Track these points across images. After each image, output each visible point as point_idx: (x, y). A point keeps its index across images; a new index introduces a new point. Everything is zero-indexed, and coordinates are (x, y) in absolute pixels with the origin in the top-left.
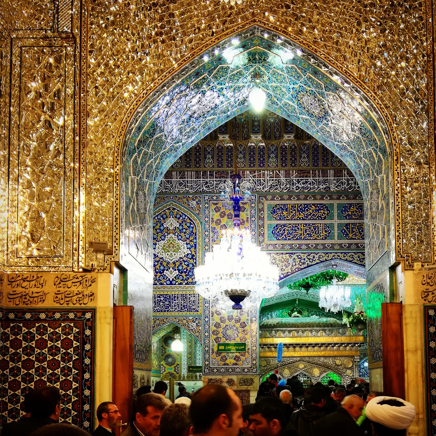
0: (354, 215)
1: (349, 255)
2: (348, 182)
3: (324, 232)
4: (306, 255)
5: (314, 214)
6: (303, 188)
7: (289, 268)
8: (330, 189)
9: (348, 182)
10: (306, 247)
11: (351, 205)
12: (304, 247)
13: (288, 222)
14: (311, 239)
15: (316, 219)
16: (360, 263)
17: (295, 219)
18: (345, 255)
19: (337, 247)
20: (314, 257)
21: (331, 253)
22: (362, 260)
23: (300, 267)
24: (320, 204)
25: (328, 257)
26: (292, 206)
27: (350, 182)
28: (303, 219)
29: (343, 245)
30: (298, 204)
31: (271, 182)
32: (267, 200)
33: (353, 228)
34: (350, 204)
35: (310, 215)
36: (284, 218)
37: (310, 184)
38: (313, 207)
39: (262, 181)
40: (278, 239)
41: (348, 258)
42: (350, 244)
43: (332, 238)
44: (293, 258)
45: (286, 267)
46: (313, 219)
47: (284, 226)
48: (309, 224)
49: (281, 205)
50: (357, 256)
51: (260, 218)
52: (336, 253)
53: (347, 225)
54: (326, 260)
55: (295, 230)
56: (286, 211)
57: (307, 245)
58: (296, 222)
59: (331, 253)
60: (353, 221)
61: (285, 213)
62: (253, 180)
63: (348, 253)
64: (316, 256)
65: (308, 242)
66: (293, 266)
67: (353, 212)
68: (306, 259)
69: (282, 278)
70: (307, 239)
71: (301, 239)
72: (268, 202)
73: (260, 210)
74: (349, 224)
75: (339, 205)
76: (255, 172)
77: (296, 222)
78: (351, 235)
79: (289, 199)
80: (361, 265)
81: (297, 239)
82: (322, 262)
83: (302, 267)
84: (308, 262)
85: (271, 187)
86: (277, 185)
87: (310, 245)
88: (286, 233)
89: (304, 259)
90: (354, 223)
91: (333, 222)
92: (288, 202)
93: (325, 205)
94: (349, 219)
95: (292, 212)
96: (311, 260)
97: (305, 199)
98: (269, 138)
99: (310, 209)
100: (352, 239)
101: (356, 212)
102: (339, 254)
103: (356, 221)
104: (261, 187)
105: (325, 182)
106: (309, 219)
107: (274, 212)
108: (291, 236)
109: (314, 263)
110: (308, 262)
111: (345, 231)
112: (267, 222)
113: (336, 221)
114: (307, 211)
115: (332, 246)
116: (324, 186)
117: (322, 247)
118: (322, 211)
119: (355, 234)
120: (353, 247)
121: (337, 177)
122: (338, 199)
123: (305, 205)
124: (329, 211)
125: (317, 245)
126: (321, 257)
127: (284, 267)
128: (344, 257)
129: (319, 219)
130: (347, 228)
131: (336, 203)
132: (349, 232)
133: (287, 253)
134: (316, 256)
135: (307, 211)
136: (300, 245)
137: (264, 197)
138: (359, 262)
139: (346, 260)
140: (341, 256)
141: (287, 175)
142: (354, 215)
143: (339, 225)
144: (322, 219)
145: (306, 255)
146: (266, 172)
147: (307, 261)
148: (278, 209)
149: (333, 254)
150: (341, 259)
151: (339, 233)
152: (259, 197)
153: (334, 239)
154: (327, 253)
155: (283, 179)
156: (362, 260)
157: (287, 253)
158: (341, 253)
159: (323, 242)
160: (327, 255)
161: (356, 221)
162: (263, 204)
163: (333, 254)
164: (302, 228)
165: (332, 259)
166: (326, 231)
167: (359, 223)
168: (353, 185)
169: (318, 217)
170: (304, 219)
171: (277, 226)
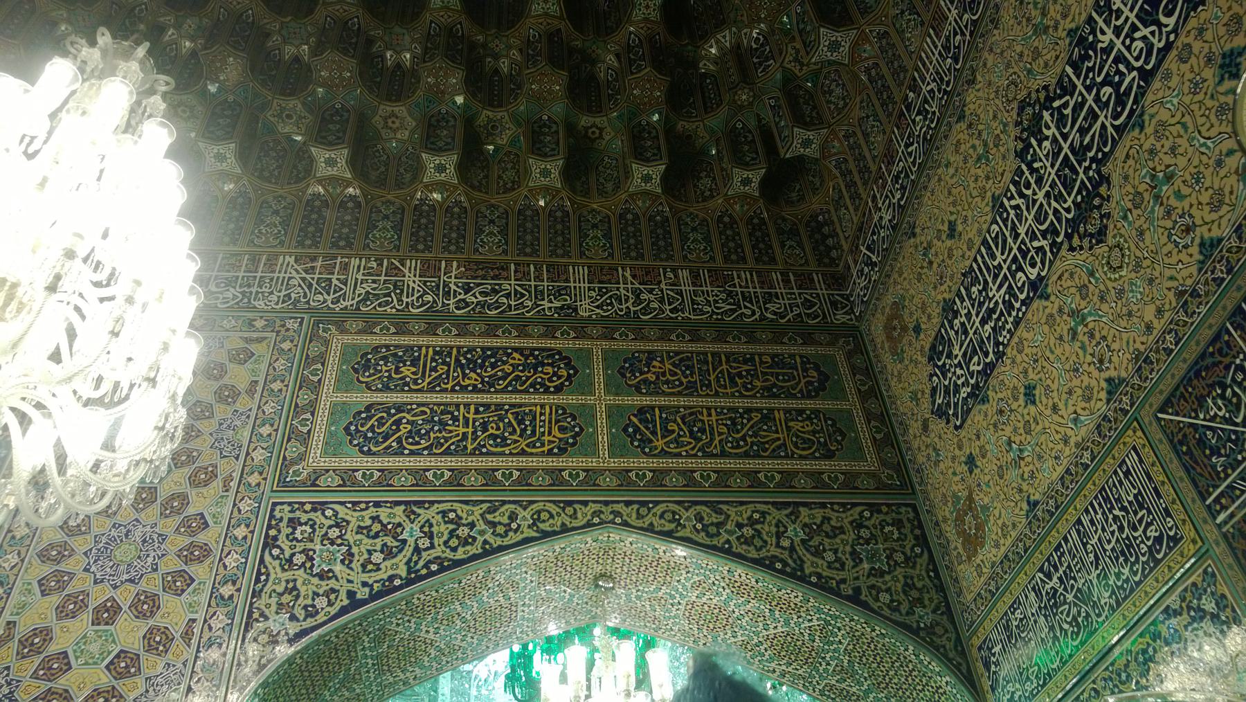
0: (667, 382)
1: (659, 509)
2: (638, 296)
3: (555, 431)
4: (478, 511)
5: (518, 378)
6: (482, 305)
7: (401, 559)
8: (575, 310)
9: (638, 296)
10: (481, 481)
11: (651, 355)
12: (472, 480)
13: (419, 398)
14: (502, 454)
15: (526, 391)
16: (708, 541)
17: (445, 390)
18: (643, 511)
19: (608, 481)
20: (513, 517)
21: (585, 503)
22: (713, 530)
23: (449, 554)
24: (542, 350)
25: (574, 516)
26: (435, 353)
27: (644, 296)
28: (475, 390)
29: (632, 475)
30: (459, 348)
31: (367, 287)
32: (343, 331)
33: (665, 422)
34: (649, 352)
35: (504, 378)
36: (403, 386)
37: (508, 296)
38: (515, 355)
39: (335, 282)
40: (369, 453)
41: (656, 521)
42: (659, 474)
43: (592, 450)
44: (422, 519)
45: (388, 553)
46: (515, 391)
47: (399, 410)
48: (499, 406)
49: (396, 347)
50: (691, 513)
51: (303, 383)
52: (606, 503)
53: (642, 411)
54: (565, 529)
55: (443, 424)
56: (412, 365)
57: (488, 473)
58: (448, 398)
59: (585, 503)
60: (662, 401)
61: (407, 371)
62: (304, 279)
63: (657, 503)
64: (522, 514)
65: (492, 462)
66: (417, 550)
67: (664, 374)
68: (481, 526)
69: (364, 602)
70: (489, 454)
71: (462, 451)
72: (348, 339)
73: (309, 361)
74: (653, 408)
75: (608, 357)
76: (314, 259)
77: (448, 398)
78: (660, 443)
79: (431, 330)
80: (714, 548)
81: (447, 453)
82: (546, 535)
83: (460, 554)
84: (488, 536)
85: (365, 300)
86: (389, 295)
87: (499, 475)
88: (404, 429)
89: (472, 525)
90: (668, 407)
91: (590, 400)
92: (423, 340)
93: (559, 353)
94: (648, 394)
95: (434, 369)
96: (501, 530)
97: (490, 332)
98: (382, 183)
99: (504, 363)
100: (664, 453)
101: (676, 374)
102: (617, 507)
103: (674, 401)
104: (330, 298)
105: (558, 293)
106: (497, 392)
107: (366, 367)
108: (424, 443)
109: (513, 538)
110: (488, 536)
111: (637, 430)
112: (329, 396)
113: (600, 400)
114: (493, 366)
115: (591, 478)
116: (558, 304)
117: (548, 480)
118: (550, 370)
119: (676, 441)
120: (674, 480)
121: (600, 282)
122: (604, 337)
123: (484, 349)
124: (573, 368)
125: (527, 473)
126: (544, 516)
127: (377, 557)
128: (639, 516)
129: (536, 391)
130: (644, 421)
131: (598, 348)
132: (654, 433)
133: (398, 503)
134: (522, 514)
135: (493, 366)
136: (458, 474)
137: (335, 323)
138: (701, 538)
139: (650, 529)
140: (630, 513)
141: (429, 269)
142: (667, 382)
143: (612, 412)
144: (547, 391)
145: (478, 511)
146: (355, 262)
147: (482, 533)
148: (385, 358)
149: (597, 507)
150: (625, 524)
151: (613, 437)
152: (317, 323)
153: (595, 453)
154: (570, 503)
155: (411, 279)
156: (713, 530)
157: (398, 503)
158: (628, 503)
159: (552, 462)
160: (569, 510)
161: (674, 401)
162: (327, 343)
163: (593, 507)
164: (471, 416)
165: (589, 525)
166: (562, 429)
167: (685, 408)
168: (655, 305)
169: (532, 385)
170: (481, 391)
171: (369, 408)
